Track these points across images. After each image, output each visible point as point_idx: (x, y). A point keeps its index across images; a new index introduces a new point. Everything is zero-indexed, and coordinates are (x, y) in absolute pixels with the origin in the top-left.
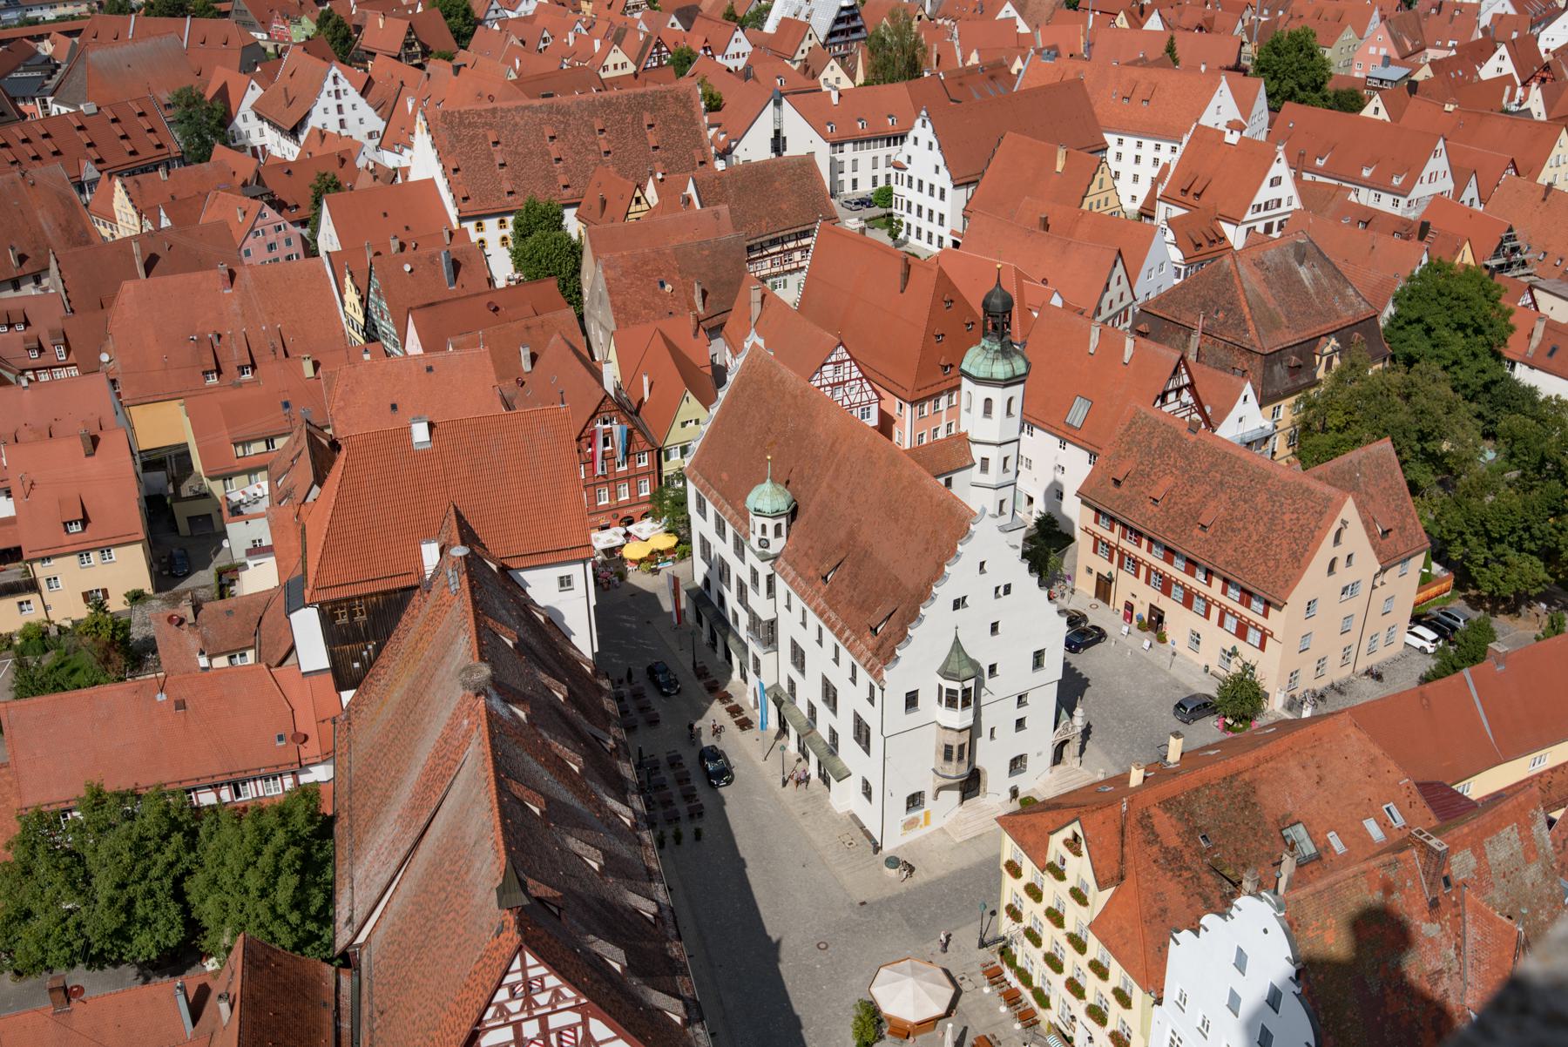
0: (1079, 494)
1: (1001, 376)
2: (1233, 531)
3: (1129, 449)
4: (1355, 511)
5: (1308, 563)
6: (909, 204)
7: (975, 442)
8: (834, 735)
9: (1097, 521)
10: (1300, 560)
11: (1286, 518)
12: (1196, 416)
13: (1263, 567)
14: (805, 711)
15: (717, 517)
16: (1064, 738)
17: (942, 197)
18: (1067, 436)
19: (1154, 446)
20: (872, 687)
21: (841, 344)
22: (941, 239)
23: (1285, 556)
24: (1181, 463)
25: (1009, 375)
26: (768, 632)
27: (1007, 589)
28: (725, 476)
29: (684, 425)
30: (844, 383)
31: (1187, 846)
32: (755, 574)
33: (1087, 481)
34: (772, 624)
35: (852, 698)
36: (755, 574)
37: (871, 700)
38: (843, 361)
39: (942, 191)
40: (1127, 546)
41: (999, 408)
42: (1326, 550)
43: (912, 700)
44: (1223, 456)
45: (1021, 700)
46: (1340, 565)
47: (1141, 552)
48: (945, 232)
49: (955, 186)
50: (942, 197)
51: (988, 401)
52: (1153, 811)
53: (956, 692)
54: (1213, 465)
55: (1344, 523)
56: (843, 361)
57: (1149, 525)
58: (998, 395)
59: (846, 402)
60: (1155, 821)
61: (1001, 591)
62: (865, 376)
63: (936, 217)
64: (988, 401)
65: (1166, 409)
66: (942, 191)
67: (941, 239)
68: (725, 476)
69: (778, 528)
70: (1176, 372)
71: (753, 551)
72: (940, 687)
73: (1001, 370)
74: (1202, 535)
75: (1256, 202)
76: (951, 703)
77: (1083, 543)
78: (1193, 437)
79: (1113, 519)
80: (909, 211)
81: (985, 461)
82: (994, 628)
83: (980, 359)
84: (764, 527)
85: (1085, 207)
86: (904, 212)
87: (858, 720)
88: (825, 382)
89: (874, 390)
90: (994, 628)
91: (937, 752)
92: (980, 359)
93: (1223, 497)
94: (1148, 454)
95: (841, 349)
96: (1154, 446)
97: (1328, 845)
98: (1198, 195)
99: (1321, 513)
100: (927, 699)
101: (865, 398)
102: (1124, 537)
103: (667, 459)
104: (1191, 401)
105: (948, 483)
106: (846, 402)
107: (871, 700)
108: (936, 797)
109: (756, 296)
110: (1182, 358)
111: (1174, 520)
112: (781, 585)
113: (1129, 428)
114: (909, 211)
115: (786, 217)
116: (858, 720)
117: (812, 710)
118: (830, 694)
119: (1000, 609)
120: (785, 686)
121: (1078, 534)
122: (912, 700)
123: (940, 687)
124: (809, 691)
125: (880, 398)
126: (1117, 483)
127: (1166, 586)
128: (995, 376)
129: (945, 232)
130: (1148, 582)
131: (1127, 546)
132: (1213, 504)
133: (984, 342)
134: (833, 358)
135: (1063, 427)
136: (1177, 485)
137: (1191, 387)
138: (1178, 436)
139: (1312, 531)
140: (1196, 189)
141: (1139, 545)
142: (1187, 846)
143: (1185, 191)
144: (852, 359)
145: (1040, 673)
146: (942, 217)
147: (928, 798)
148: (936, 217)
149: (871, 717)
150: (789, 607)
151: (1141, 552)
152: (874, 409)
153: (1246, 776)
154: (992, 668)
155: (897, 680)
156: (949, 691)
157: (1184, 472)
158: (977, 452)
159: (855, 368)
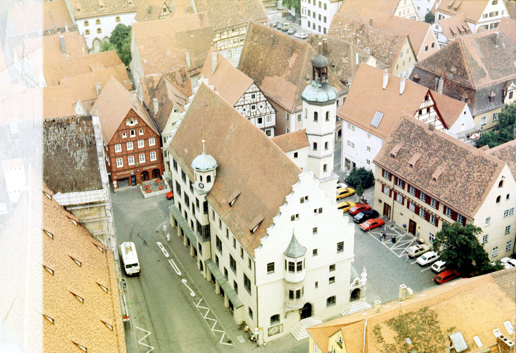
0: (374, 162)
1: (321, 100)
2: (449, 181)
3: (400, 139)
4: (509, 172)
5: (485, 198)
6: (309, 11)
7: (309, 134)
8: (236, 285)
9: (383, 175)
10: (480, 197)
11: (475, 174)
12: (439, 123)
13: (463, 200)
14: (223, 272)
15: (183, 172)
16: (356, 287)
17: (325, 8)
18: (372, 131)
19: (412, 137)
20: (250, 260)
21: (254, 83)
22: (325, 29)
23: (474, 194)
24: (425, 146)
25: (326, 100)
26: (205, 232)
27: (321, 211)
28: (186, 151)
29: (173, 124)
30: (257, 103)
31: (398, 343)
32: (197, 201)
33: (378, 156)
34: (208, 227)
35: (242, 265)
36: (197, 201)
37: (250, 266)
38: (256, 92)
39: (325, 5)
40: (398, 188)
41: (322, 116)
42: (494, 191)
43: (271, 267)
44: (447, 145)
45: (332, 267)
46: (503, 199)
47: (405, 192)
48: (327, 25)
49: (331, 2)
50: (325, 8)
51: (316, 114)
52: (381, 325)
53: (293, 264)
54: (440, 147)
55: (503, 177)
56: (256, 92)
57: (408, 178)
58: (322, 111)
59: (258, 113)
60: (382, 331)
61: (318, 211)
62: (267, 100)
63: (322, 18)
64: (316, 114)
65: (421, 118)
66: (325, 5)
67: (325, 29)
68: (186, 151)
69: (209, 179)
70: (426, 98)
71: (196, 189)
72: (286, 261)
73: (322, 96)
74: (433, 183)
75: (485, 13)
76: (291, 268)
77: (378, 186)
78: (431, 133)
79: (390, 175)
80: (309, 15)
81: (315, 145)
82: (315, 230)
83: (312, 90)
84: (201, 177)
85: (397, 14)
86: (307, 15)
87: (245, 277)
88: (246, 103)
89: (273, 107)
90: (315, 230)
91: (286, 293)
92: (312, 90)
93: (445, 163)
94: (408, 141)
95: (254, 86)
96: (412, 137)
97: (474, 344)
98: (456, 9)
99: (492, 172)
100: (279, 267)
101: (268, 111)
102: (396, 184)
103: (165, 141)
104: (435, 113)
105: (296, 155)
106: (258, 113)
107: (250, 266)
108: (286, 317)
109: (214, 58)
110: (429, 92)
111: (420, 175)
112: (210, 208)
113: (400, 127)
114: (309, 15)
115: (241, 18)
116: (245, 277)
117: (226, 272)
118: (233, 263)
119: (317, 220)
120: (214, 259)
121: (376, 183)
122: (271, 267)
123: (286, 261)
124: (225, 262)
125: (276, 111)
126: (393, 156)
127: (417, 210)
128: (319, 100)
129: (327, 25)
130: (408, 207)
131: (398, 188)
132: (440, 167)
133: (314, 83)
134: (251, 90)
135: (369, 127)
136: (422, 157)
137: (435, 106)
138: (424, 133)
139: (487, 182)
140: (455, 6)
141: (403, 188)
142: (398, 343)
143: (450, 7)
144: (260, 91)
145: (341, 254)
146: (325, 18)
147: (282, 318)
148: (322, 18)
149: (251, 278)
150: (214, 218)
151: (405, 192)
152: (273, 116)
153: (432, 308)
154: (315, 252)
155: (262, 257)
156: (290, 263)
157: (426, 150)
158: (312, 140)
159: (262, 96)
